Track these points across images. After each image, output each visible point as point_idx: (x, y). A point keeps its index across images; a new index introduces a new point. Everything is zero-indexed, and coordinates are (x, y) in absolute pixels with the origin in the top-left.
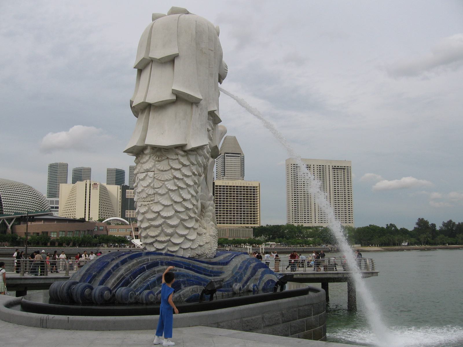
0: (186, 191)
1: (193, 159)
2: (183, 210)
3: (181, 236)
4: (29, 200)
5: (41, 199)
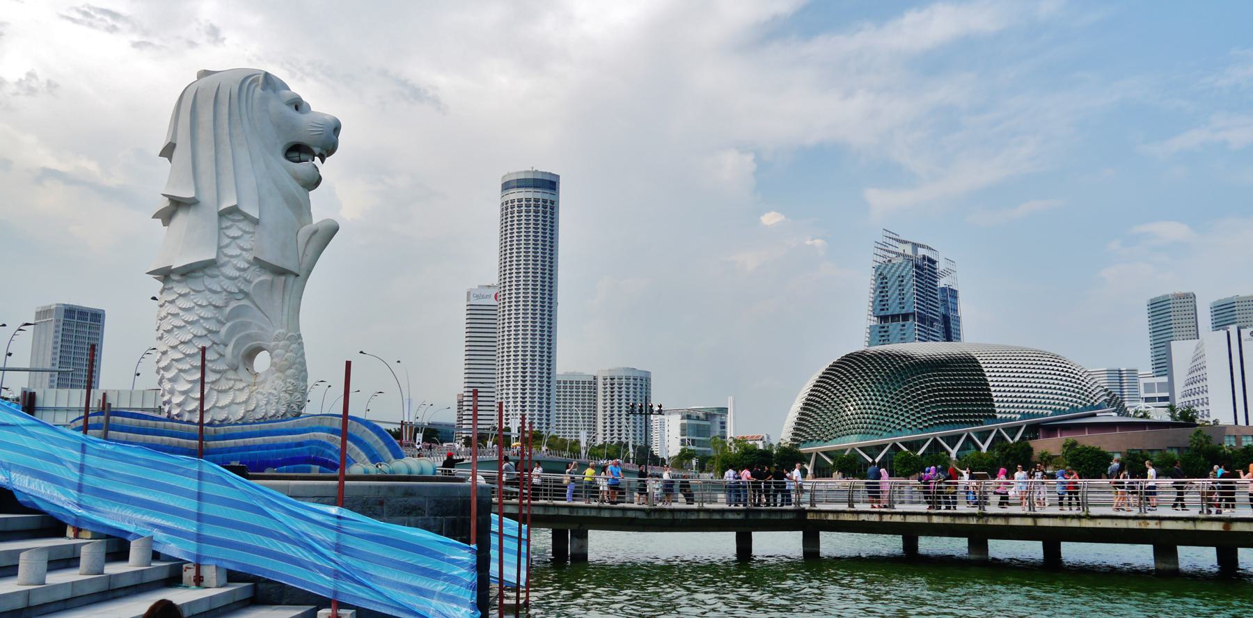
4: (1053, 384)
5: (1083, 381)
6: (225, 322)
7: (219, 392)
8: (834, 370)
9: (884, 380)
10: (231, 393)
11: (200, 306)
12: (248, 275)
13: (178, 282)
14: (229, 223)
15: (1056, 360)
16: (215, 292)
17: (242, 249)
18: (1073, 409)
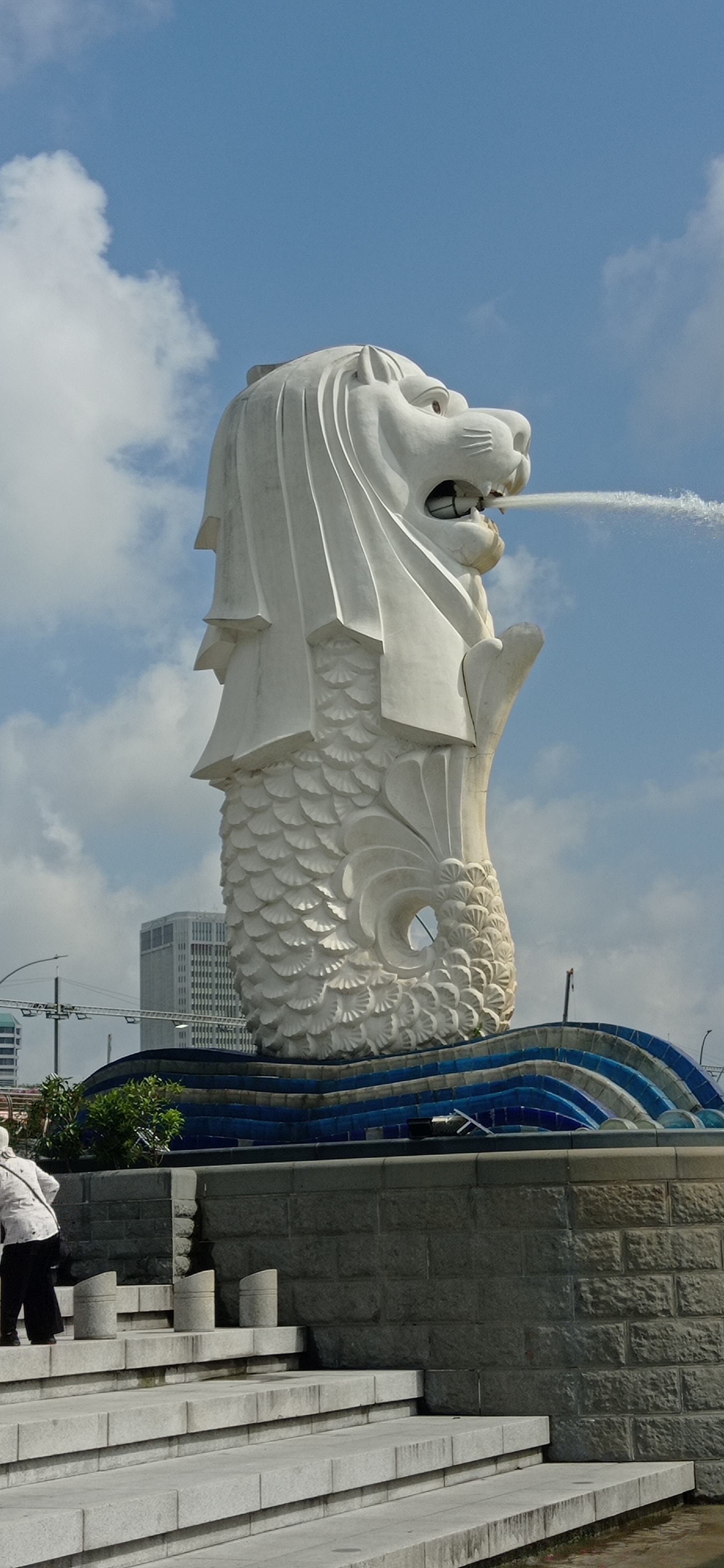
6: (342, 854)
7: (345, 993)
11: (290, 827)
16: (312, 797)
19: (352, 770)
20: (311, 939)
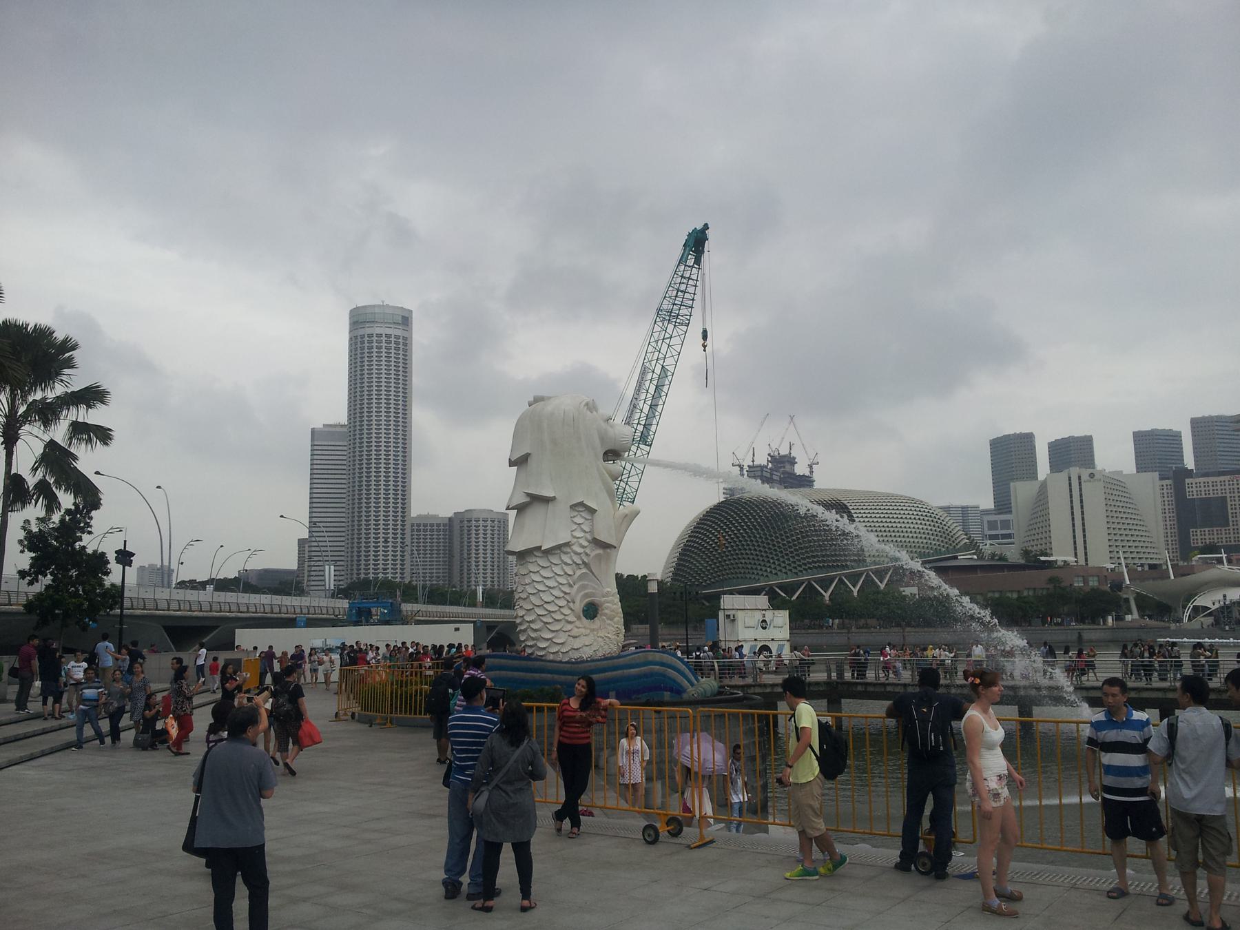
0: (548, 593)
1: (555, 560)
2: (546, 613)
3: (547, 640)
8: (712, 517)
9: (760, 525)
10: (582, 637)
12: (588, 551)
13: (541, 557)
14: (576, 513)
15: (920, 506)
17: (585, 532)
18: (937, 552)
19: (582, 555)
20: (563, 617)
